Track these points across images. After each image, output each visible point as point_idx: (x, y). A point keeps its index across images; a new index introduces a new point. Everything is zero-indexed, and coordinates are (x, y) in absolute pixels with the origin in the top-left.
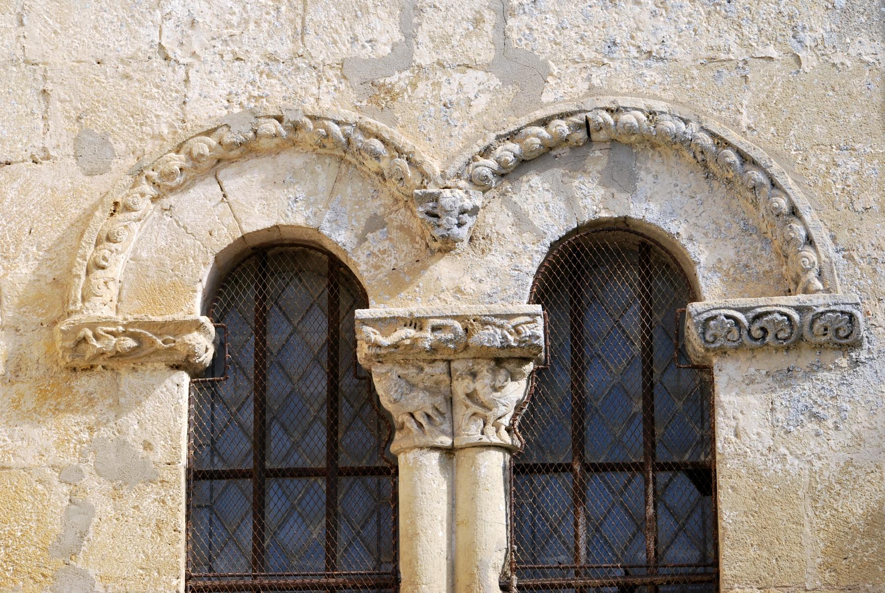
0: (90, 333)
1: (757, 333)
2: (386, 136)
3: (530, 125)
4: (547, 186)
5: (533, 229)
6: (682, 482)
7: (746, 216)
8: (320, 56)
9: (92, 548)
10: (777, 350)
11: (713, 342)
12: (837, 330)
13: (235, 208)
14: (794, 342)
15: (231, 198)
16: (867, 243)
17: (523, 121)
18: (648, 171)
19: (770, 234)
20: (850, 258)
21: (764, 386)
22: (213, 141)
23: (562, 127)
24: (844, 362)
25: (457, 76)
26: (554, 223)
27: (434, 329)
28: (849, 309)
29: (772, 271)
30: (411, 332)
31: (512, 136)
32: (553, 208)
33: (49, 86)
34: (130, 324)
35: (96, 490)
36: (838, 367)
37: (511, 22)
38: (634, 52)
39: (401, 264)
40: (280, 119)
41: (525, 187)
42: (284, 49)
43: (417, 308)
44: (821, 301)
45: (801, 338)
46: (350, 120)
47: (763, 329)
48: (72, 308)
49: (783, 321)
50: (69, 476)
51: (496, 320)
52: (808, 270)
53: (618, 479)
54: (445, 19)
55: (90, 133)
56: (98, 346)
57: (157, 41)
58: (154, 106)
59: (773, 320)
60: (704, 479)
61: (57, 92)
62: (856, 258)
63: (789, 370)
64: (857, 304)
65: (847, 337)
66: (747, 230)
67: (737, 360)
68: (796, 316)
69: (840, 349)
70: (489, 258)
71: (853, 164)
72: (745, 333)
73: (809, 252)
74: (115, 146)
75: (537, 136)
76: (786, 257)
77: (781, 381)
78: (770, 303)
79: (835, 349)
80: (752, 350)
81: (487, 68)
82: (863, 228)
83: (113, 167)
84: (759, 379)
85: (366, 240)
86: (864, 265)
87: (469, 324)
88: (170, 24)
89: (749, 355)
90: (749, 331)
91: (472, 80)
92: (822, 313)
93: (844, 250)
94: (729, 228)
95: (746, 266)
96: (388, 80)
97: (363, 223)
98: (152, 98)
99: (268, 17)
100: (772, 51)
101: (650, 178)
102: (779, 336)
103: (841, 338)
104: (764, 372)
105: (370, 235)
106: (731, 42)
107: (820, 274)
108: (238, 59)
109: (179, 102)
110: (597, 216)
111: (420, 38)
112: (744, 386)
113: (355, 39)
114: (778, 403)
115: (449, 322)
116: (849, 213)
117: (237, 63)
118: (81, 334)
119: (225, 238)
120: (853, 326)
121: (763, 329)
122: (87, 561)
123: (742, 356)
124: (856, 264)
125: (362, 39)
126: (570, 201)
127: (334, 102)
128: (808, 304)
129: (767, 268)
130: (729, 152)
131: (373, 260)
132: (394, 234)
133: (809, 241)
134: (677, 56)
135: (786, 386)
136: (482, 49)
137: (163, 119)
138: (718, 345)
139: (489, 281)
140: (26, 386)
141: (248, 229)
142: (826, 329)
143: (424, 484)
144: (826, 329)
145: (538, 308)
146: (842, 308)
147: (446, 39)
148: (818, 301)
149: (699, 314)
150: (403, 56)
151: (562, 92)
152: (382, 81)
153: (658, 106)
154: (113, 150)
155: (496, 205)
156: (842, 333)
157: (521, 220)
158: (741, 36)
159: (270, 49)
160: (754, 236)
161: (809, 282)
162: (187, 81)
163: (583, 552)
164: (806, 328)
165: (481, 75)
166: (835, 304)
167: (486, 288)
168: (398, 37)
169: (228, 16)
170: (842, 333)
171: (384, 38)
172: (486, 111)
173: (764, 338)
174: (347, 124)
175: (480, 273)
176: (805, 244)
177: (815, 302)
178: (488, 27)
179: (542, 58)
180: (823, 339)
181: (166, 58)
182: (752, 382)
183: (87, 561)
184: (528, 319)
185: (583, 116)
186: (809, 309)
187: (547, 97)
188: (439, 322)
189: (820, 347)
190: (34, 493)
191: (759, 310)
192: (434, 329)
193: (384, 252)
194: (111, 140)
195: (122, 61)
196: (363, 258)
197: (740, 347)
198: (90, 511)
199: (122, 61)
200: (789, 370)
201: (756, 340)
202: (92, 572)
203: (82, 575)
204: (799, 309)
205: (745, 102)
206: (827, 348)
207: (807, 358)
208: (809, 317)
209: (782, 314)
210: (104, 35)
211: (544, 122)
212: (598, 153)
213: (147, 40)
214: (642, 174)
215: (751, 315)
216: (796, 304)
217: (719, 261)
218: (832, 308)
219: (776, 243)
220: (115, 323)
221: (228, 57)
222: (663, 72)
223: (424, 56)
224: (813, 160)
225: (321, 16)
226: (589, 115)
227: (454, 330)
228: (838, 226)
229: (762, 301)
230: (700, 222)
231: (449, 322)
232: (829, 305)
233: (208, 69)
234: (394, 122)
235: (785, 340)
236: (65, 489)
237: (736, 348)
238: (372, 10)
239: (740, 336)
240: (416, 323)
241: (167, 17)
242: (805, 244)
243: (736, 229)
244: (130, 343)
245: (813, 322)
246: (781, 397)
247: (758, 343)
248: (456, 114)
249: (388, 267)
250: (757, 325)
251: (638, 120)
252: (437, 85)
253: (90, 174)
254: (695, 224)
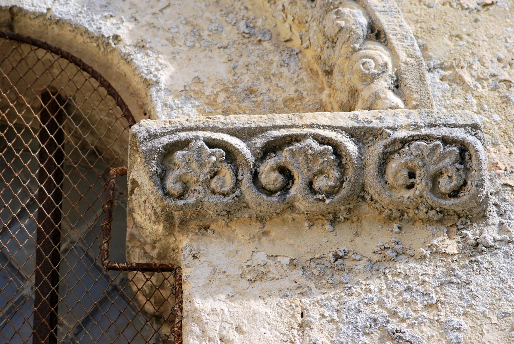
1: (270, 177)
7: (251, 15)
10: (312, 220)
11: (181, 197)
12: (435, 178)
14: (346, 200)
16: (488, 56)
19: (297, 41)
20: (459, 81)
21: (287, 283)
24: (452, 246)
28: (458, 133)
29: (301, 98)
36: (436, 252)
44: (402, 120)
45: (360, 194)
47: (283, 170)
49: (323, 154)
52: (375, 77)
59: (304, 152)
62: (467, 78)
63: (337, 257)
64: (475, 126)
65: (455, 194)
66: (251, 34)
67: (230, 240)
68: (351, 147)
69: (440, 222)
72: (246, 177)
73: (378, 52)
76: (329, 73)
77: (320, 276)
78: (297, 121)
79: (428, 221)
80: (261, 219)
82: (481, 34)
84: (274, 272)
86: (483, 91)
89: (256, 228)
90: (255, 176)
92: (405, 142)
93: (442, 67)
94: (218, 31)
95: (250, 91)
102: (317, 185)
103: (443, 196)
104: (287, 261)
107: (397, 86)
112: (244, 284)
114: (314, 313)
116: (451, 12)
120: (467, 170)
121: (283, 170)
123: (241, 233)
124: (467, 88)
128: (376, 124)
129: (291, 92)
133: (375, 33)
135: (332, 286)
138: (191, 200)
142: (412, 175)
144: (412, 175)
146: (445, 131)
148: (395, 117)
149: (153, 136)
156: (445, 185)
160: (266, 45)
161: (376, 96)
164: (372, 170)
166: (431, 125)
170: (445, 185)
173: (285, 189)
176: (367, 38)
177: (390, 121)
180: (407, 194)
182: (261, 277)
186: (376, 134)
189: (398, 217)
191: (275, 133)
197: (234, 211)
200: (337, 257)
201: (271, 193)
204: (358, 135)
206: (413, 221)
207: (372, 238)
208: (377, 148)
209: (323, 141)
215: (259, 142)
216: (351, 124)
217: (198, 80)
218: (425, 131)
219: (310, 54)
228: (431, 31)
229: (280, 119)
230: (161, 21)
232: (417, 127)
235: (330, 193)
237: (229, 214)
239: (237, 183)
242: (367, 38)
243: (230, 34)
245: (385, 160)
246: (318, 304)
247: (274, 199)
250: (271, 162)
254: (152, 26)
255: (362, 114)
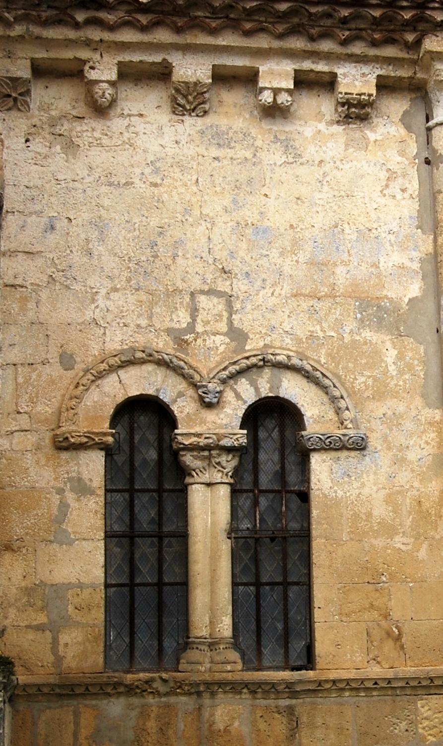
0: (69, 436)
2: (186, 360)
3: (242, 359)
4: (248, 382)
5: (243, 399)
6: (294, 498)
8: (158, 326)
9: (69, 521)
13: (125, 386)
15: (123, 382)
17: (239, 357)
18: (286, 378)
22: (116, 359)
23: (254, 360)
25: (213, 337)
26: (250, 397)
27: (206, 438)
28: (362, 436)
30: (196, 439)
31: (234, 363)
32: (247, 392)
33: (49, 333)
34: (85, 433)
35: (70, 497)
37: (234, 316)
38: (281, 331)
39: (191, 411)
40: (143, 352)
41: (239, 383)
42: (144, 322)
43: (197, 429)
46: (172, 354)
48: (61, 425)
50: (60, 491)
51: (229, 436)
53: (271, 496)
54: (208, 314)
55: (65, 353)
56: (73, 441)
57: (93, 317)
58: (93, 344)
60: (304, 497)
61: (53, 336)
68: (342, 438)
70: (225, 410)
71: (363, 379)
74: (76, 359)
75: (244, 363)
81: (225, 334)
83: (76, 367)
84: (327, 461)
85: (177, 401)
87: (220, 437)
88: (98, 310)
91: (219, 339)
92: (352, 437)
96: (186, 337)
97: (176, 394)
98: (90, 340)
99: (138, 309)
100: (333, 334)
101: (286, 381)
105: (178, 399)
106: (318, 329)
108: (126, 326)
109: (102, 342)
110: (267, 395)
111: (198, 321)
113: (172, 320)
115: (211, 436)
117: (125, 328)
118: (65, 436)
119: (120, 398)
121: (330, 442)
122: (67, 525)
125: (175, 320)
126: (257, 389)
127: (163, 345)
128: (347, 433)
130: (318, 372)
131: (179, 409)
132: (188, 399)
133: (347, 409)
134: (298, 334)
136: (223, 327)
137: (95, 349)
139: (227, 421)
140: (41, 455)
141: (130, 395)
143: (197, 496)
145: (245, 432)
146: (359, 435)
147: (208, 322)
148: (351, 433)
150: (191, 328)
151: (253, 345)
152: (183, 338)
153: (291, 354)
154: (75, 361)
155: (228, 389)
157: (238, 396)
158: (322, 328)
159: (138, 323)
162: (105, 334)
163: (258, 525)
165: (222, 337)
167: (224, 422)
168: (190, 320)
169: (122, 308)
171: (184, 321)
172: (224, 352)
174: (171, 355)
175: (222, 416)
177: (351, 433)
178: (225, 319)
179: (246, 332)
181: (97, 324)
182: (325, 462)
183: (67, 525)
184: (242, 435)
185: (263, 356)
187: (247, 348)
188: (208, 436)
190: (46, 498)
192: (206, 438)
193: (184, 406)
194: (74, 356)
195: (79, 324)
196: (176, 408)
198: (68, 506)
199: (79, 324)
202: (70, 530)
203: (65, 531)
204: (344, 435)
205: (323, 353)
208: (347, 438)
210: (70, 313)
211: (247, 358)
212: (267, 371)
213: (89, 316)
214: (284, 379)
215: (326, 436)
217: (313, 415)
220: (79, 432)
221: (122, 325)
222: (292, 340)
223: (199, 328)
224: (348, 377)
225: (158, 310)
226: (265, 356)
227: (213, 439)
231: (211, 436)
233: (113, 329)
234: (187, 354)
236: (58, 497)
238: (179, 309)
240: (198, 435)
241: (97, 307)
244: (85, 440)
248: (212, 353)
249: (186, 412)
250: (329, 440)
251: (284, 359)
252: (204, 340)
253: (66, 370)
255: (344, 430)
